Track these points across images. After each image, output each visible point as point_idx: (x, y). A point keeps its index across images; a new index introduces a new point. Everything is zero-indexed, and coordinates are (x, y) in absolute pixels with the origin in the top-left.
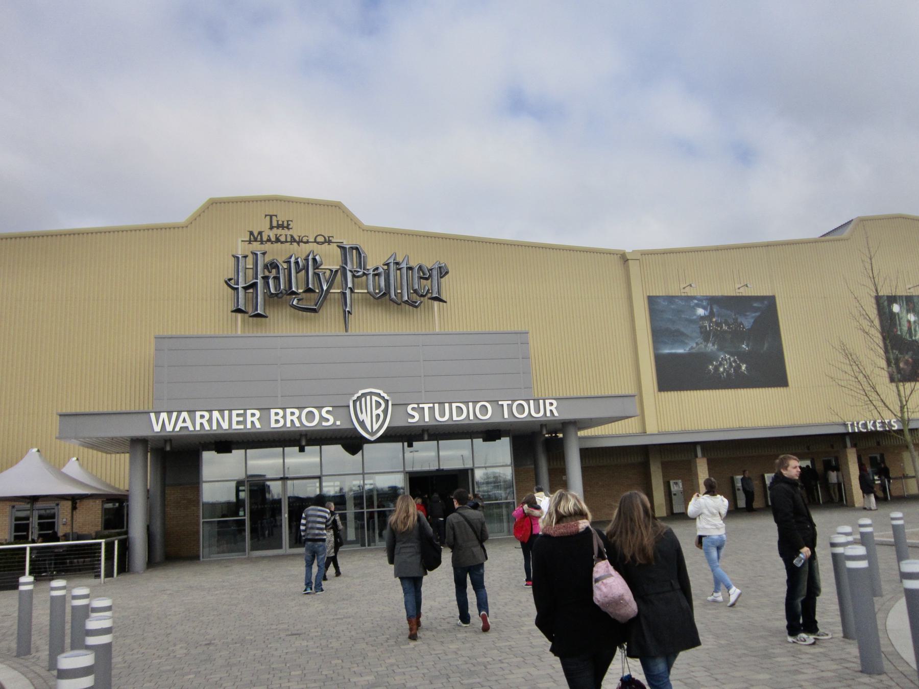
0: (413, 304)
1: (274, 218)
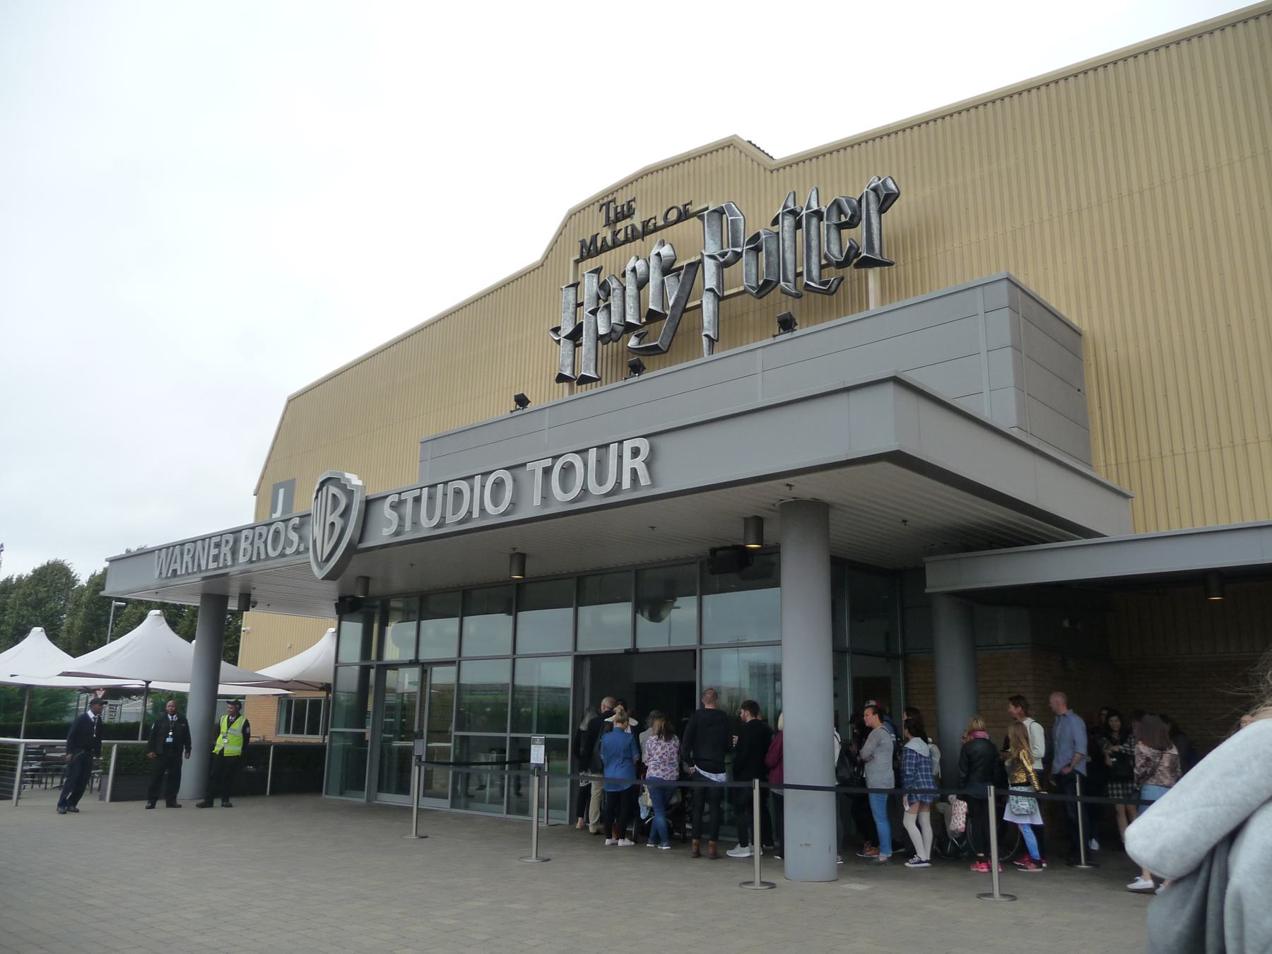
0: (828, 290)
1: (612, 205)
